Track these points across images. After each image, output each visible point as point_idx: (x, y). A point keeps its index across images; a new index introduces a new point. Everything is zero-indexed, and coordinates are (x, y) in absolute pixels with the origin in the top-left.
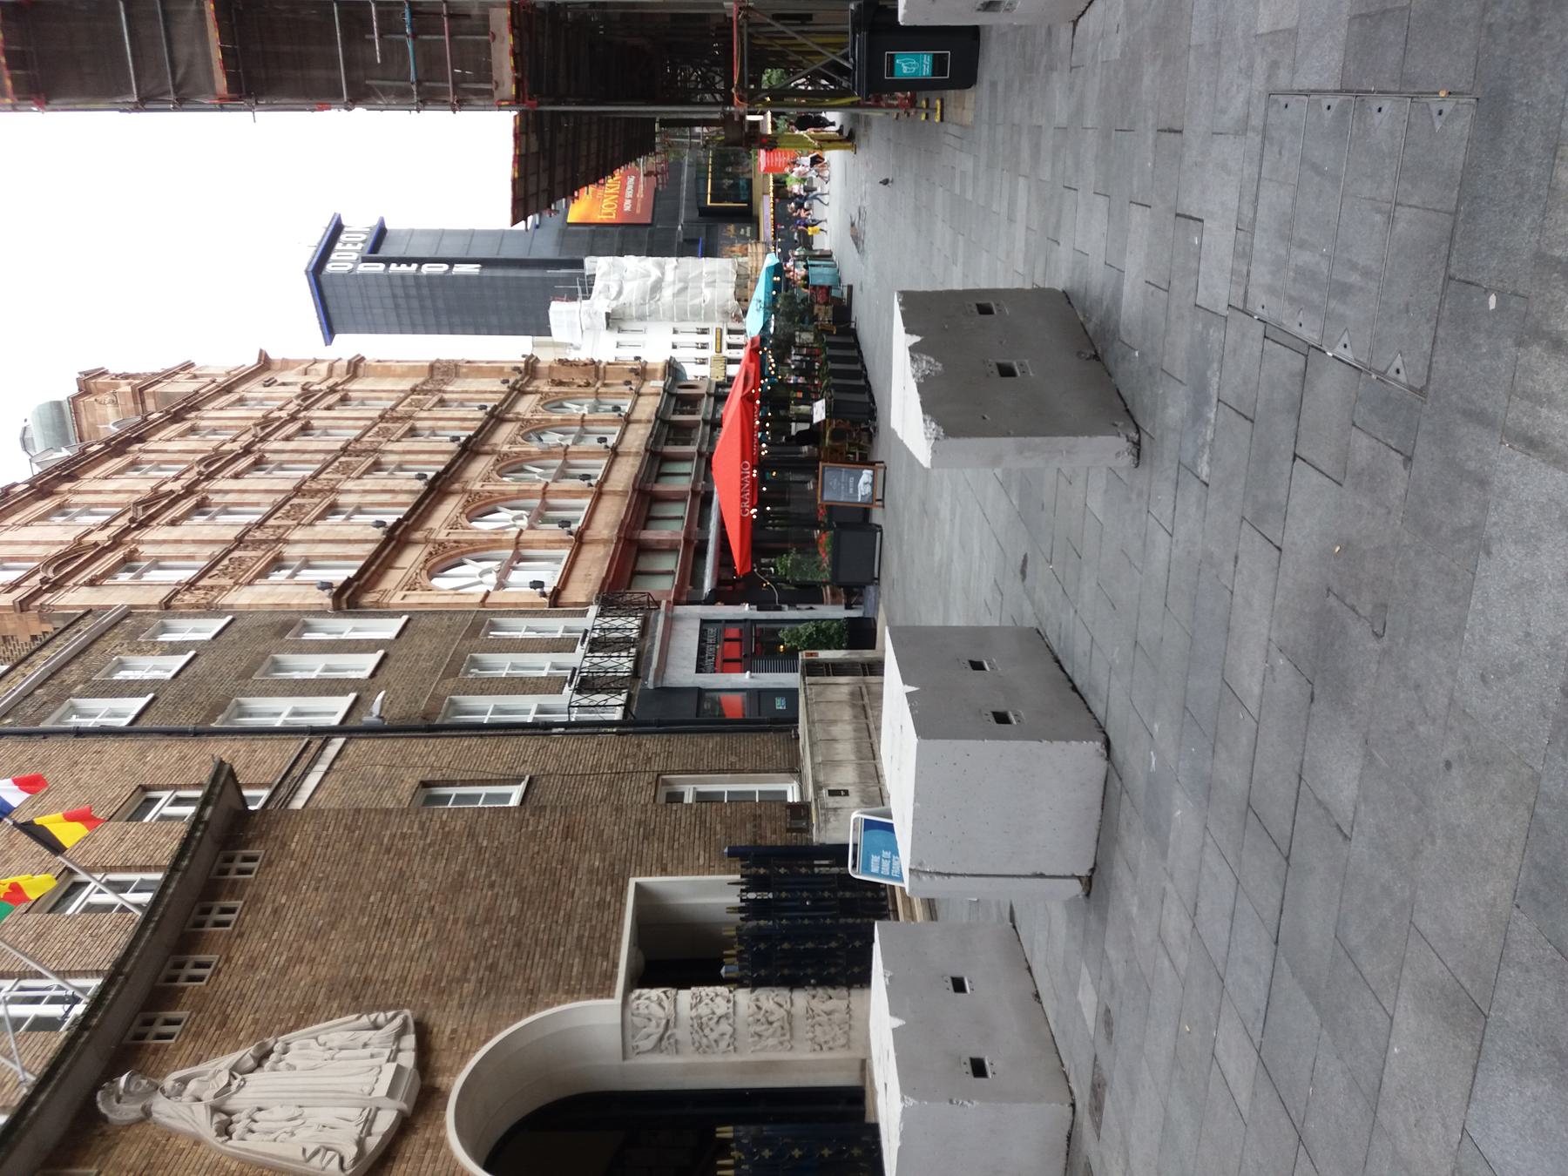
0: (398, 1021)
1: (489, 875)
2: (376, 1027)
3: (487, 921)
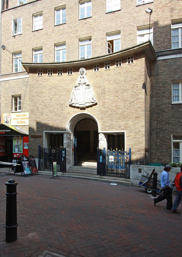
0: (93, 101)
1: (127, 105)
3: (117, 108)
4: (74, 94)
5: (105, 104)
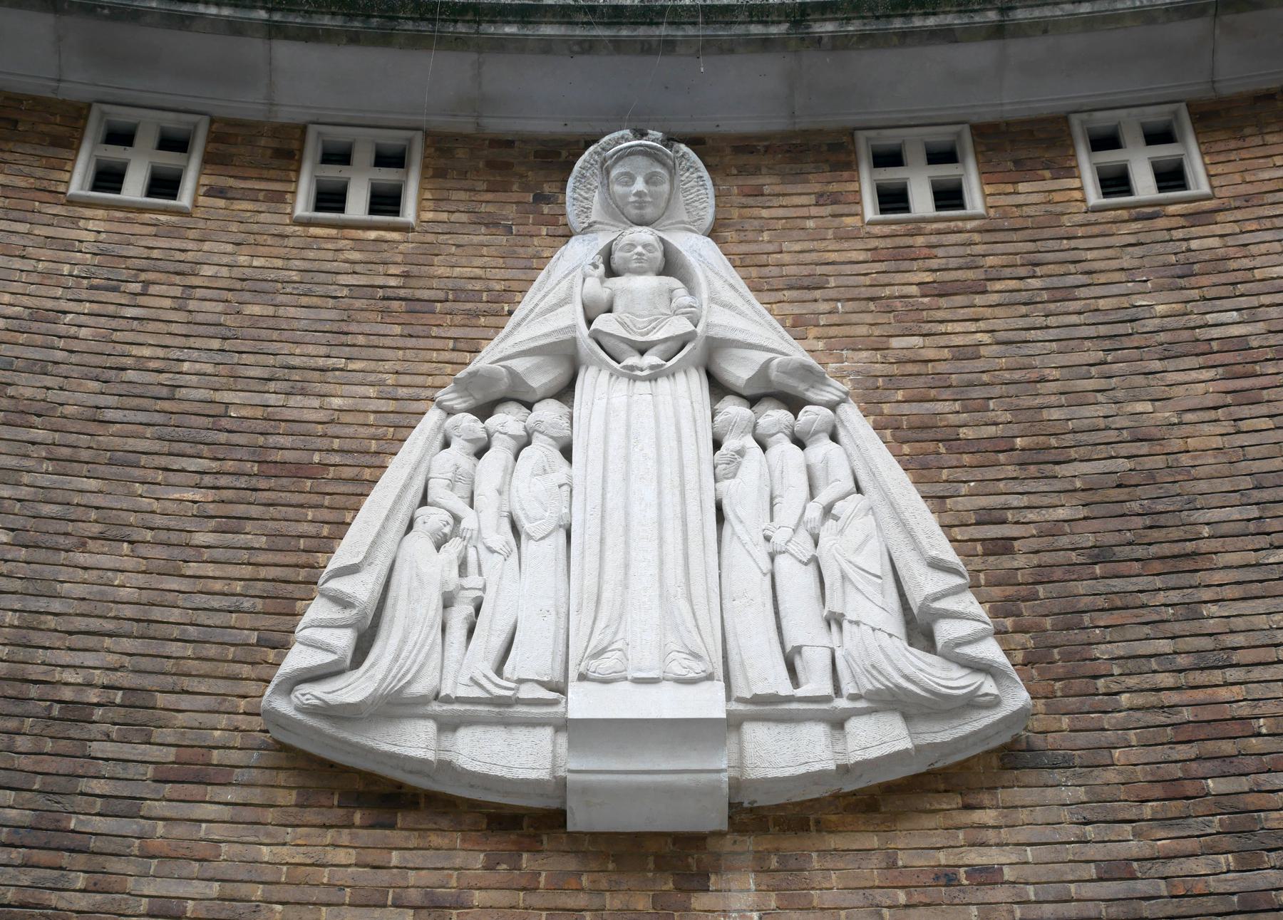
0: (957, 681)
2: (919, 630)
4: (433, 518)
5: (1227, 766)
